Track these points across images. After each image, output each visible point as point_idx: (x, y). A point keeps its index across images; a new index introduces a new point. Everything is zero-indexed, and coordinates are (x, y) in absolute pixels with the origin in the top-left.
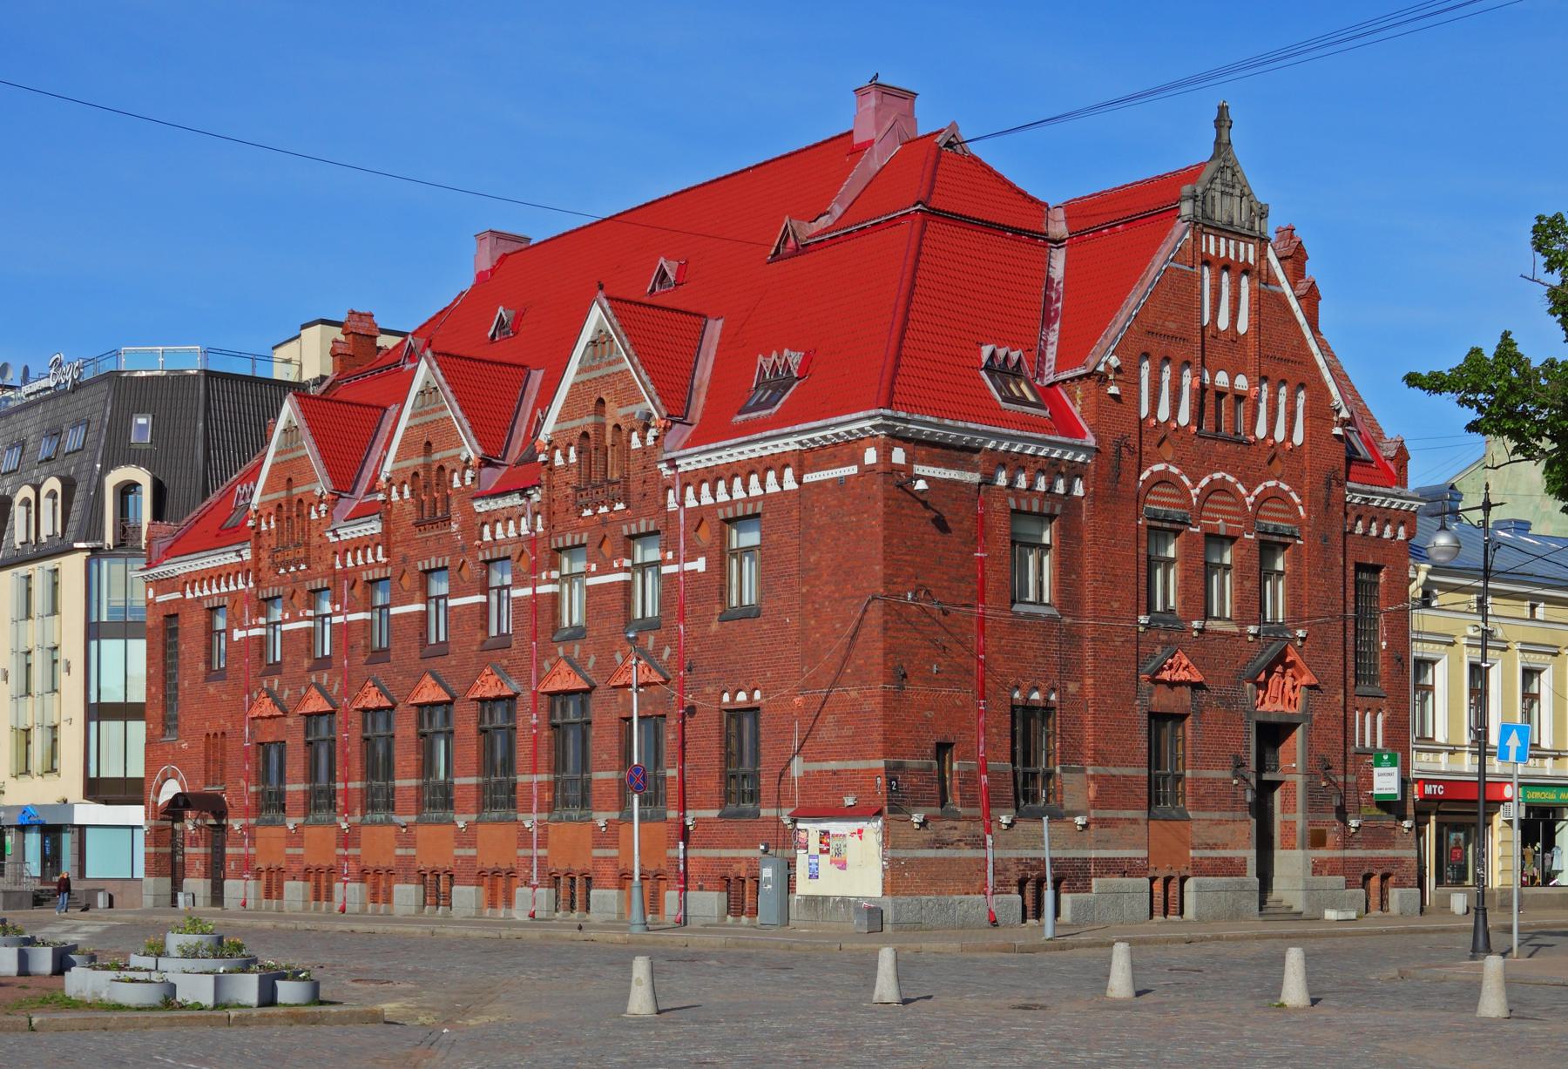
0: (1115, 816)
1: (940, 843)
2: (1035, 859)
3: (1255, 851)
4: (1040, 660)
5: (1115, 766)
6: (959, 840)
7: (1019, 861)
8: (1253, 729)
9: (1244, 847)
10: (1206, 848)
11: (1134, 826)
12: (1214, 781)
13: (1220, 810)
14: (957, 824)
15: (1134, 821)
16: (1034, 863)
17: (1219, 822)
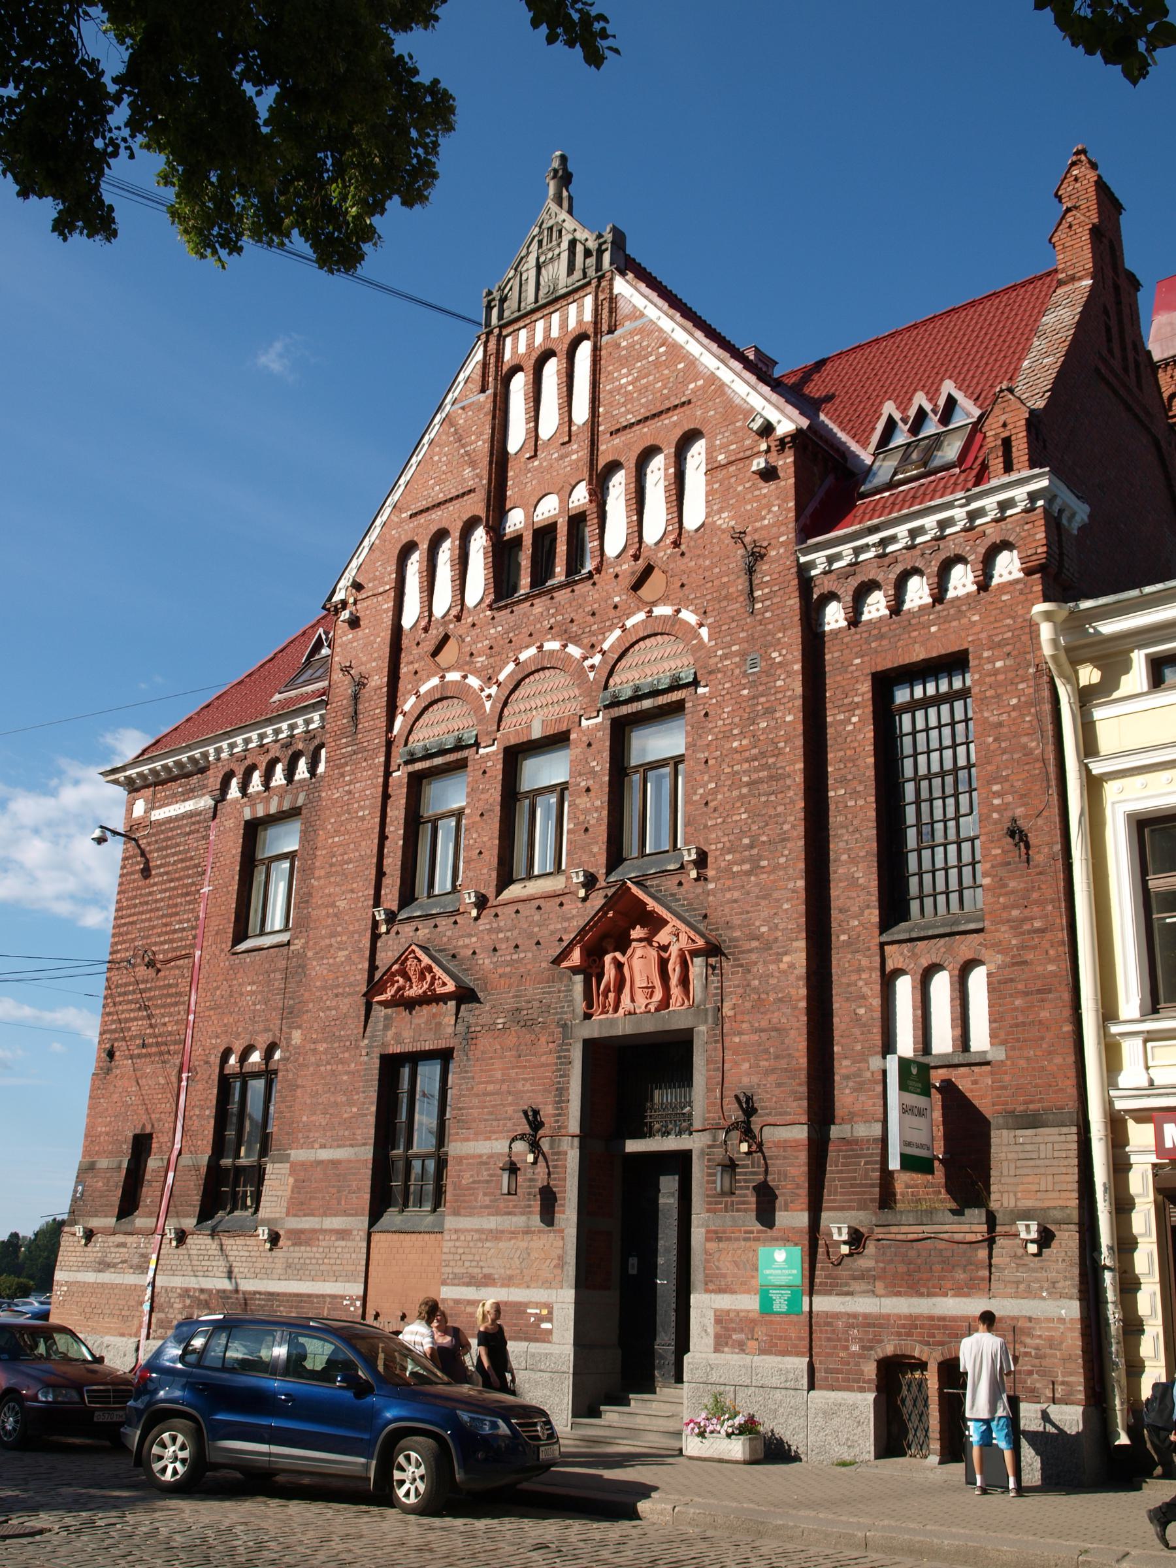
0: (318, 1227)
1: (104, 1265)
2: (202, 1291)
3: (572, 1292)
4: (258, 1007)
5: (323, 1146)
6: (123, 1262)
7: (186, 1293)
8: (577, 1055)
9: (547, 1284)
10: (468, 1284)
11: (343, 1243)
12: (483, 1162)
13: (497, 1213)
14: (130, 1239)
15: (343, 1234)
16: (202, 1297)
17: (496, 1235)
